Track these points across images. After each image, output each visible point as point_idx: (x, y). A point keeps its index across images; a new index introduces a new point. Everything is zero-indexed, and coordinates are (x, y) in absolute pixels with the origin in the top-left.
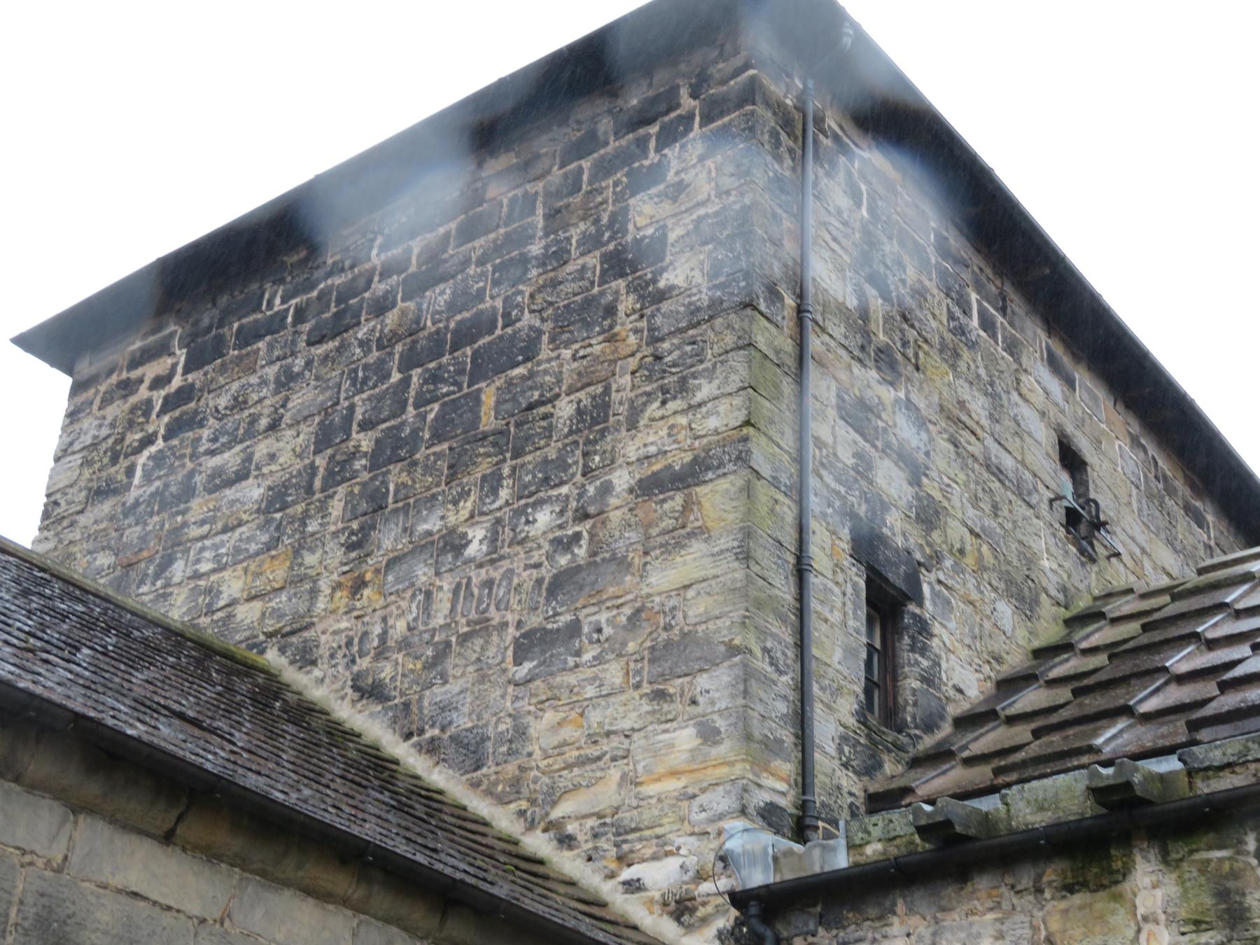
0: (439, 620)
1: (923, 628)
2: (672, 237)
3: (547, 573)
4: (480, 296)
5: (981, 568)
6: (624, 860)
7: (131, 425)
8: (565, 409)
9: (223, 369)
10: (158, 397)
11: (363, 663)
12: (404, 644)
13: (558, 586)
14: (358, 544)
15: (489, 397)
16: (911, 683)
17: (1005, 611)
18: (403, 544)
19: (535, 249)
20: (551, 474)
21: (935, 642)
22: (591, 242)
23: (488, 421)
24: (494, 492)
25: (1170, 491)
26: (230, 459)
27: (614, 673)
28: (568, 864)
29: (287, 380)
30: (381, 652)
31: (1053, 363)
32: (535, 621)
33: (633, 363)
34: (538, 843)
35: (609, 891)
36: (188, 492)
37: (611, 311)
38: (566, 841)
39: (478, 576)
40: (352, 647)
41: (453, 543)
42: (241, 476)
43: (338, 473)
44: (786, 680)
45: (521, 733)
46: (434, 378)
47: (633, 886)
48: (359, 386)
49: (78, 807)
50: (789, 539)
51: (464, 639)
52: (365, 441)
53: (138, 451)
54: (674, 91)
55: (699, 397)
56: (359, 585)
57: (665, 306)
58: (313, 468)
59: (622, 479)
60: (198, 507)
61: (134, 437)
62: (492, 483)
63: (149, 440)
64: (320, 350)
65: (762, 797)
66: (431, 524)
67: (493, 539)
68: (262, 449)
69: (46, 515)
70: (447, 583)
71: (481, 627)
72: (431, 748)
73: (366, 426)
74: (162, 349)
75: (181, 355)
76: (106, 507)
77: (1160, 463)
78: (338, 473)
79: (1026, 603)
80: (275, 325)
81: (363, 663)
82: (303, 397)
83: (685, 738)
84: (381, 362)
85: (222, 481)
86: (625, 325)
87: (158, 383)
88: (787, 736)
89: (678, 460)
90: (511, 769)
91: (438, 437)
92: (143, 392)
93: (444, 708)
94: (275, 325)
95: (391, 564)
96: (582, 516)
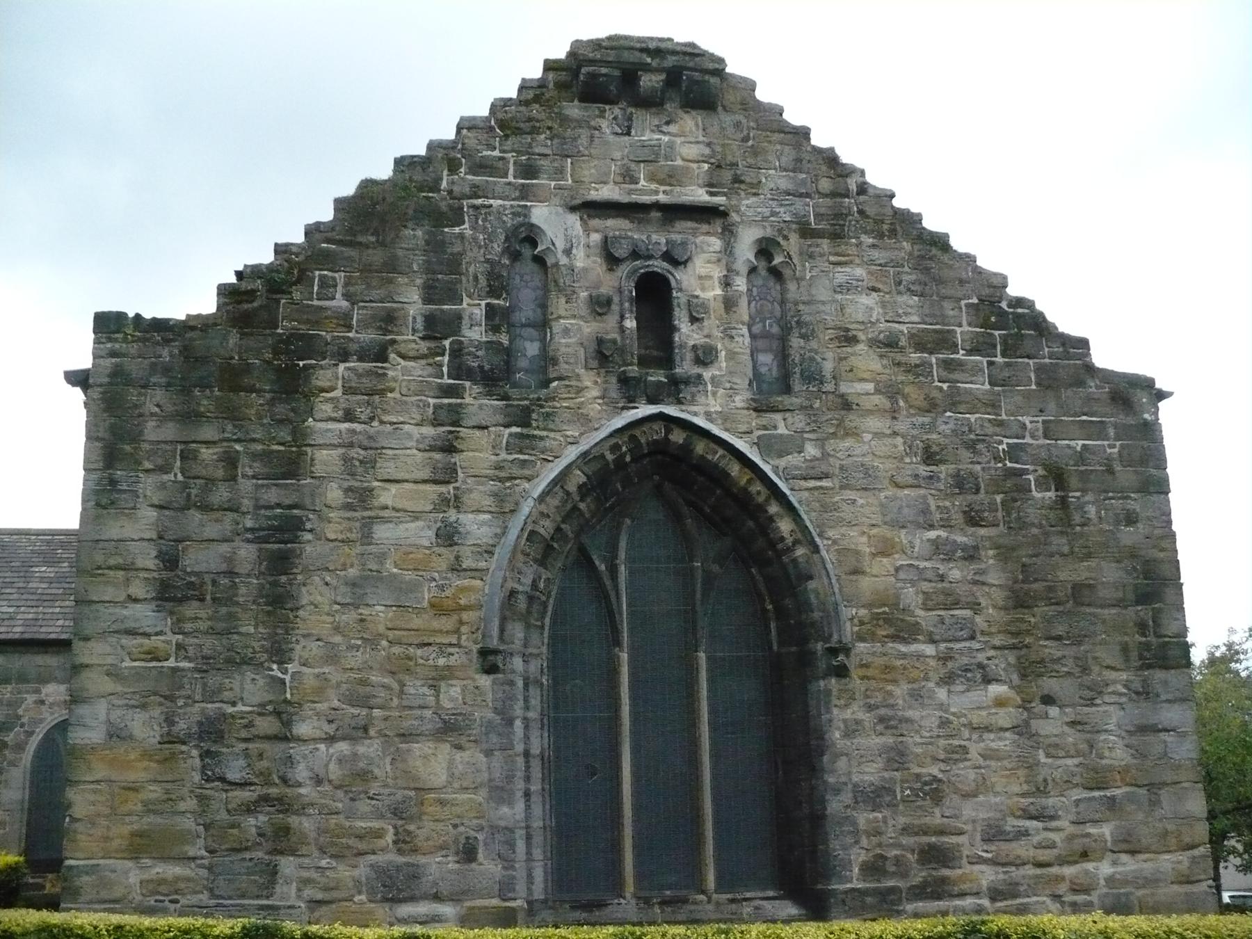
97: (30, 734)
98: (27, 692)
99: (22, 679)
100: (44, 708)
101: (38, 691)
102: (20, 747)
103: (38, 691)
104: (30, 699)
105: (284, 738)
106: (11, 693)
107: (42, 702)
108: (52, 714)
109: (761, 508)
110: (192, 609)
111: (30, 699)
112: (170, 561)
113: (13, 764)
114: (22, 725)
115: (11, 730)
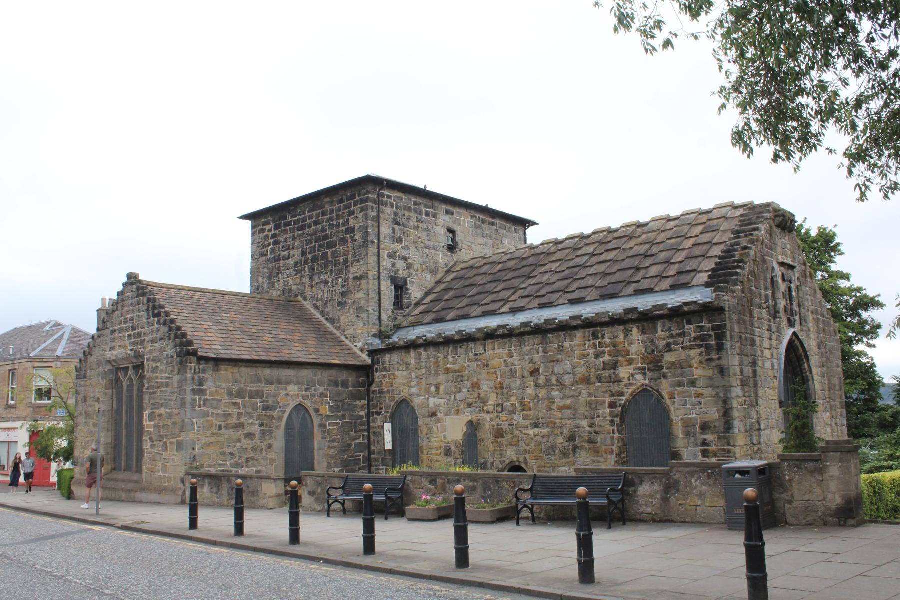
0: (326, 296)
1: (408, 290)
2: (356, 228)
3: (341, 291)
4: (326, 231)
5: (423, 270)
6: (355, 342)
7: (265, 240)
8: (342, 259)
9: (282, 232)
10: (270, 234)
11: (315, 302)
12: (321, 300)
13: (344, 294)
14: (311, 278)
15: (330, 254)
16: (405, 301)
17: (429, 277)
18: (319, 281)
19: (335, 222)
20: (341, 272)
21: (410, 292)
22: (344, 225)
23: (330, 259)
24: (331, 274)
25: (484, 222)
26: (286, 253)
27: (352, 311)
28: (347, 342)
29: (294, 238)
30: (317, 301)
31: (448, 212)
32: (340, 300)
33: (351, 253)
34: (343, 338)
35: (353, 346)
36: (279, 260)
37: (348, 241)
38: (347, 338)
39: (331, 289)
40: (313, 299)
41: (326, 282)
42: (289, 258)
43: (306, 262)
44: (377, 313)
45: (339, 319)
46: (320, 246)
47: (356, 346)
48: (308, 244)
49: (278, 368)
50: (377, 288)
51: (330, 301)
52: (310, 257)
53: (268, 247)
54: (355, 195)
55: (362, 263)
56: (312, 287)
57: (356, 243)
58: (301, 260)
59: (351, 277)
60: (282, 263)
61: (267, 243)
62: (331, 271)
63: (270, 245)
64: (300, 233)
65: (372, 334)
66: (323, 277)
67: (332, 283)
68: (292, 253)
69: (252, 257)
70: (326, 290)
71: (332, 300)
72: (327, 319)
73: (310, 254)
74: (268, 223)
75: (273, 225)
76: (264, 258)
77: (481, 217)
78: (306, 262)
79: (434, 272)
80: (290, 224)
81: (315, 302)
82: (297, 243)
83: (361, 324)
84: (311, 239)
85: (285, 259)
86: (350, 245)
87: (270, 231)
88: (377, 322)
89: (359, 275)
90: (338, 325)
91: (322, 260)
92: (267, 233)
93: (328, 313)
94: (290, 224)
95: (318, 283)
96: (345, 282)
97: (284, 412)
98: (282, 390)
99: (280, 382)
100: (289, 398)
101: (286, 389)
102: (280, 419)
103: (286, 389)
104: (283, 393)
105: (759, 430)
106: (275, 390)
107: (288, 395)
108: (293, 401)
109: (803, 360)
110: (746, 389)
111: (283, 393)
112: (742, 372)
113: (278, 428)
114: (280, 408)
115: (276, 409)
